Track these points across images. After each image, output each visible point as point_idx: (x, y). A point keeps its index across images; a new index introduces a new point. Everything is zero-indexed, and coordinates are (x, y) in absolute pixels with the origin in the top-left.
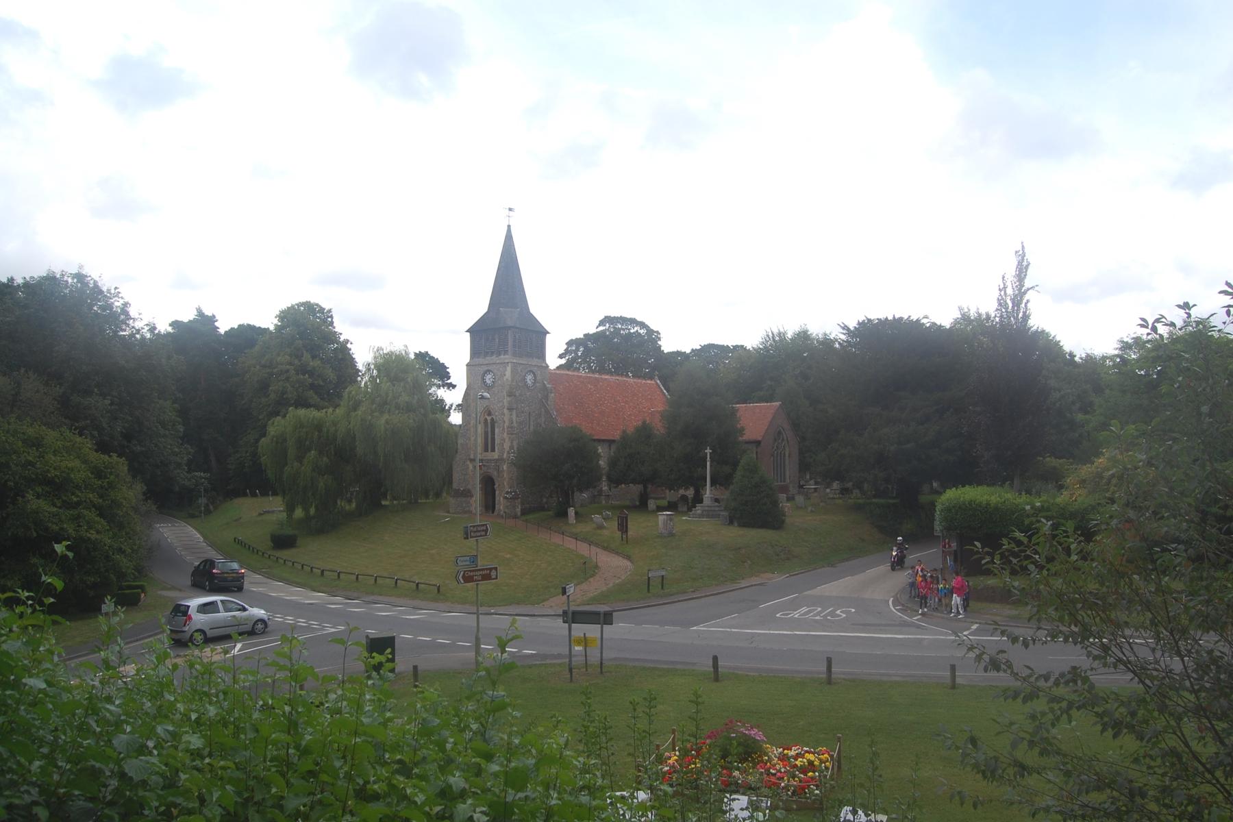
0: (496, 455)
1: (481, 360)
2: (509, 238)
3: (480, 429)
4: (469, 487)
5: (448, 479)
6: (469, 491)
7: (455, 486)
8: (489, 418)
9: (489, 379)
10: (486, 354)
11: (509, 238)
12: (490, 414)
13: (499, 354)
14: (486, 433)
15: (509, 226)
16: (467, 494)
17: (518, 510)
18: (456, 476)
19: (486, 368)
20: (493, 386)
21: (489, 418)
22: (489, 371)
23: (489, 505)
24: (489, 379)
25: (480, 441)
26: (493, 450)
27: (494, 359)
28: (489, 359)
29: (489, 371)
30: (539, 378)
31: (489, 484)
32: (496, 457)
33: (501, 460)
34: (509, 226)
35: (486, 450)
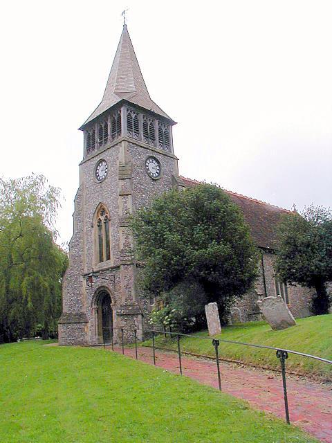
0: (111, 263)
4: (83, 310)
6: (81, 315)
7: (65, 309)
8: (103, 218)
15: (125, 26)
16: (81, 319)
18: (67, 299)
19: (97, 159)
22: (102, 160)
23: (106, 332)
25: (94, 250)
26: (108, 258)
29: (102, 160)
34: (125, 26)
35: (101, 260)
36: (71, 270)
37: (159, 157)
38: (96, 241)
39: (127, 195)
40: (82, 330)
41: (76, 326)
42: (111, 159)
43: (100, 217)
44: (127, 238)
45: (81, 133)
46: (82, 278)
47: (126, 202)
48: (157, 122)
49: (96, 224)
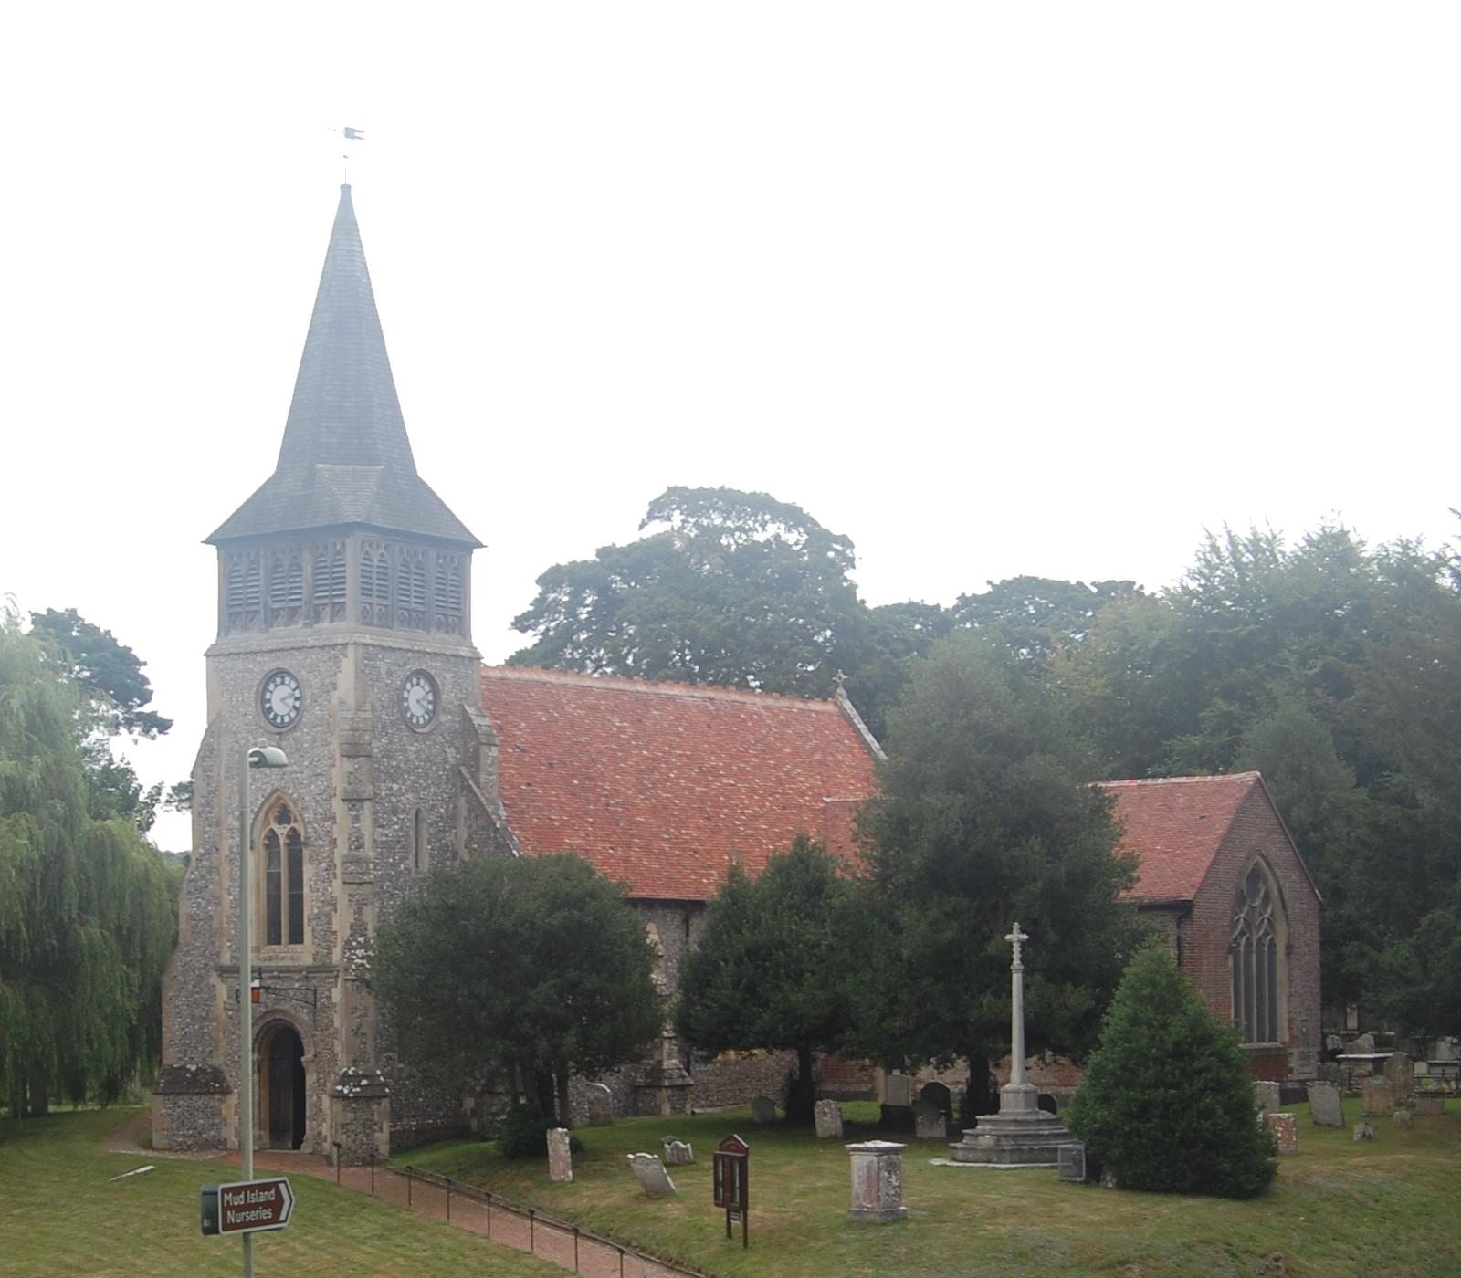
0: (305, 954)
1: (254, 638)
2: (346, 230)
3: (254, 863)
4: (217, 1061)
5: (145, 1031)
8: (282, 831)
9: (281, 699)
10: (272, 616)
11: (346, 230)
12: (284, 816)
13: (317, 619)
14: (273, 880)
16: (211, 1083)
17: (382, 1138)
19: (270, 664)
20: (294, 725)
21: (282, 831)
22: (282, 673)
23: (285, 1122)
24: (281, 699)
26: (297, 937)
27: (298, 632)
28: (281, 634)
29: (282, 673)
30: (448, 696)
31: (282, 1051)
32: (307, 960)
33: (322, 969)
35: (274, 938)
36: (187, 954)
37: (433, 666)
38: (258, 885)
39: (363, 800)
40: (216, 1113)
41: (198, 1101)
42: (316, 681)
43: (275, 826)
44: (359, 912)
45: (212, 550)
46: (214, 978)
47: (356, 819)
48: (433, 553)
49: (260, 841)
